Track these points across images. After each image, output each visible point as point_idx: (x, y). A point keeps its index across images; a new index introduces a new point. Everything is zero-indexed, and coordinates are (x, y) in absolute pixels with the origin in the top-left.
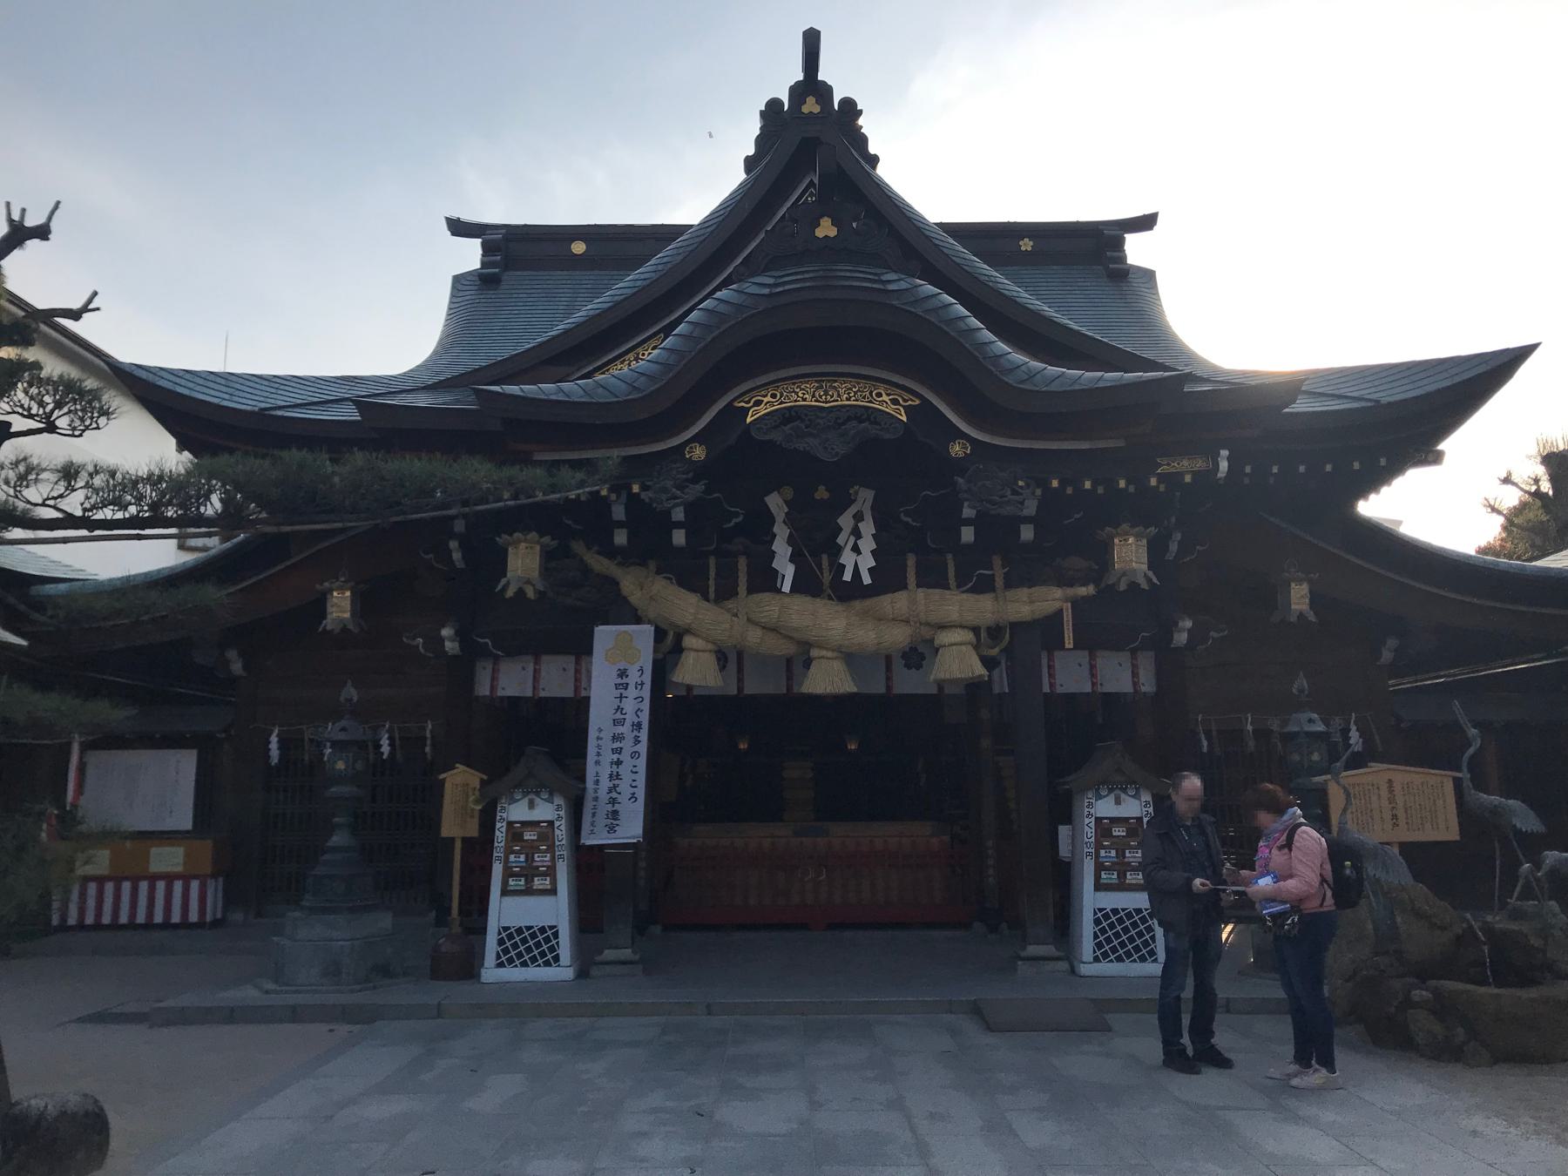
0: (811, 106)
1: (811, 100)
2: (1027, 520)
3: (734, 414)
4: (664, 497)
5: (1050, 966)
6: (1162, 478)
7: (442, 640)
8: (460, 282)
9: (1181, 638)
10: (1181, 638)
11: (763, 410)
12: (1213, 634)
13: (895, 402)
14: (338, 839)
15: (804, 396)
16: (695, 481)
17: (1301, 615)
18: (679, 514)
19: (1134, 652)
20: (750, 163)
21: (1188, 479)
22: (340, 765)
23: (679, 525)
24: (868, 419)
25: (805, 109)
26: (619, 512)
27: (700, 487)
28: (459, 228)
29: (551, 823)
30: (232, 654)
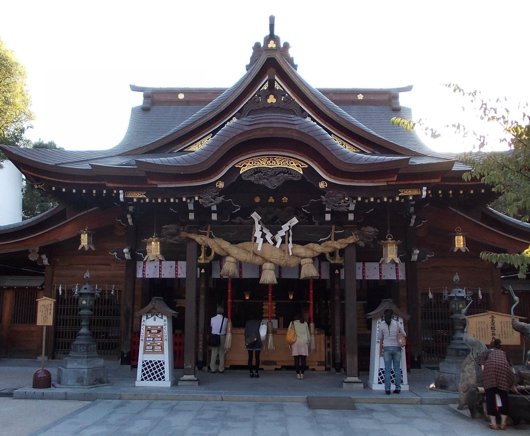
0: (272, 44)
1: (272, 42)
2: (351, 212)
4: (207, 202)
5: (356, 385)
6: (401, 197)
7: (124, 254)
8: (135, 111)
9: (415, 258)
10: (415, 258)
11: (246, 168)
12: (428, 256)
13: (298, 166)
14: (84, 330)
15: (263, 164)
17: (459, 250)
18: (214, 208)
20: (248, 67)
21: (411, 198)
22: (84, 302)
23: (214, 212)
24: (287, 173)
25: (270, 46)
26: (191, 207)
27: (221, 198)
28: (135, 89)
29: (162, 327)
30: (44, 257)
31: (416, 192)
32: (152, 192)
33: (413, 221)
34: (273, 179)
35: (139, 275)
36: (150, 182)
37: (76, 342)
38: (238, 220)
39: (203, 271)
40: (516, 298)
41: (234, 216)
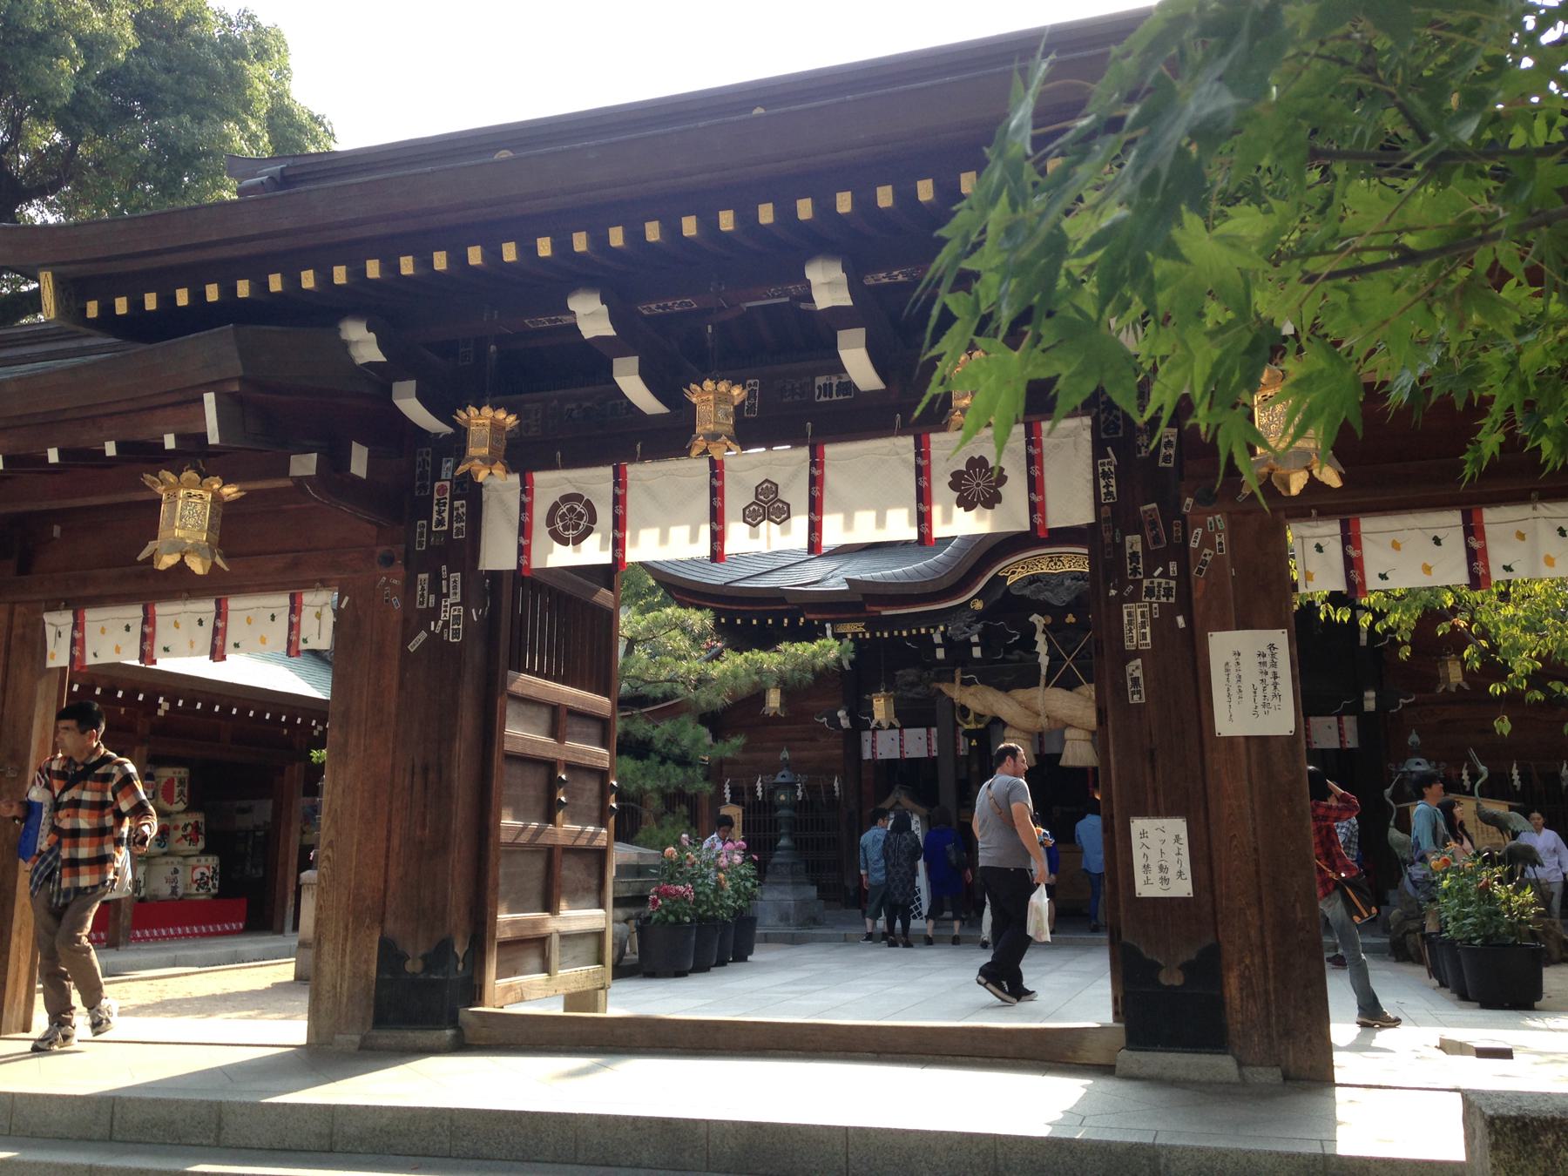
3: (998, 580)
9: (1370, 705)
10: (1370, 705)
11: (1016, 577)
14: (783, 842)
15: (1043, 568)
16: (977, 622)
18: (975, 639)
19: (1339, 716)
22: (783, 798)
23: (976, 645)
32: (874, 623)
35: (867, 755)
36: (869, 608)
37: (775, 860)
38: (1016, 655)
39: (974, 743)
40: (1483, 768)
41: (1009, 649)
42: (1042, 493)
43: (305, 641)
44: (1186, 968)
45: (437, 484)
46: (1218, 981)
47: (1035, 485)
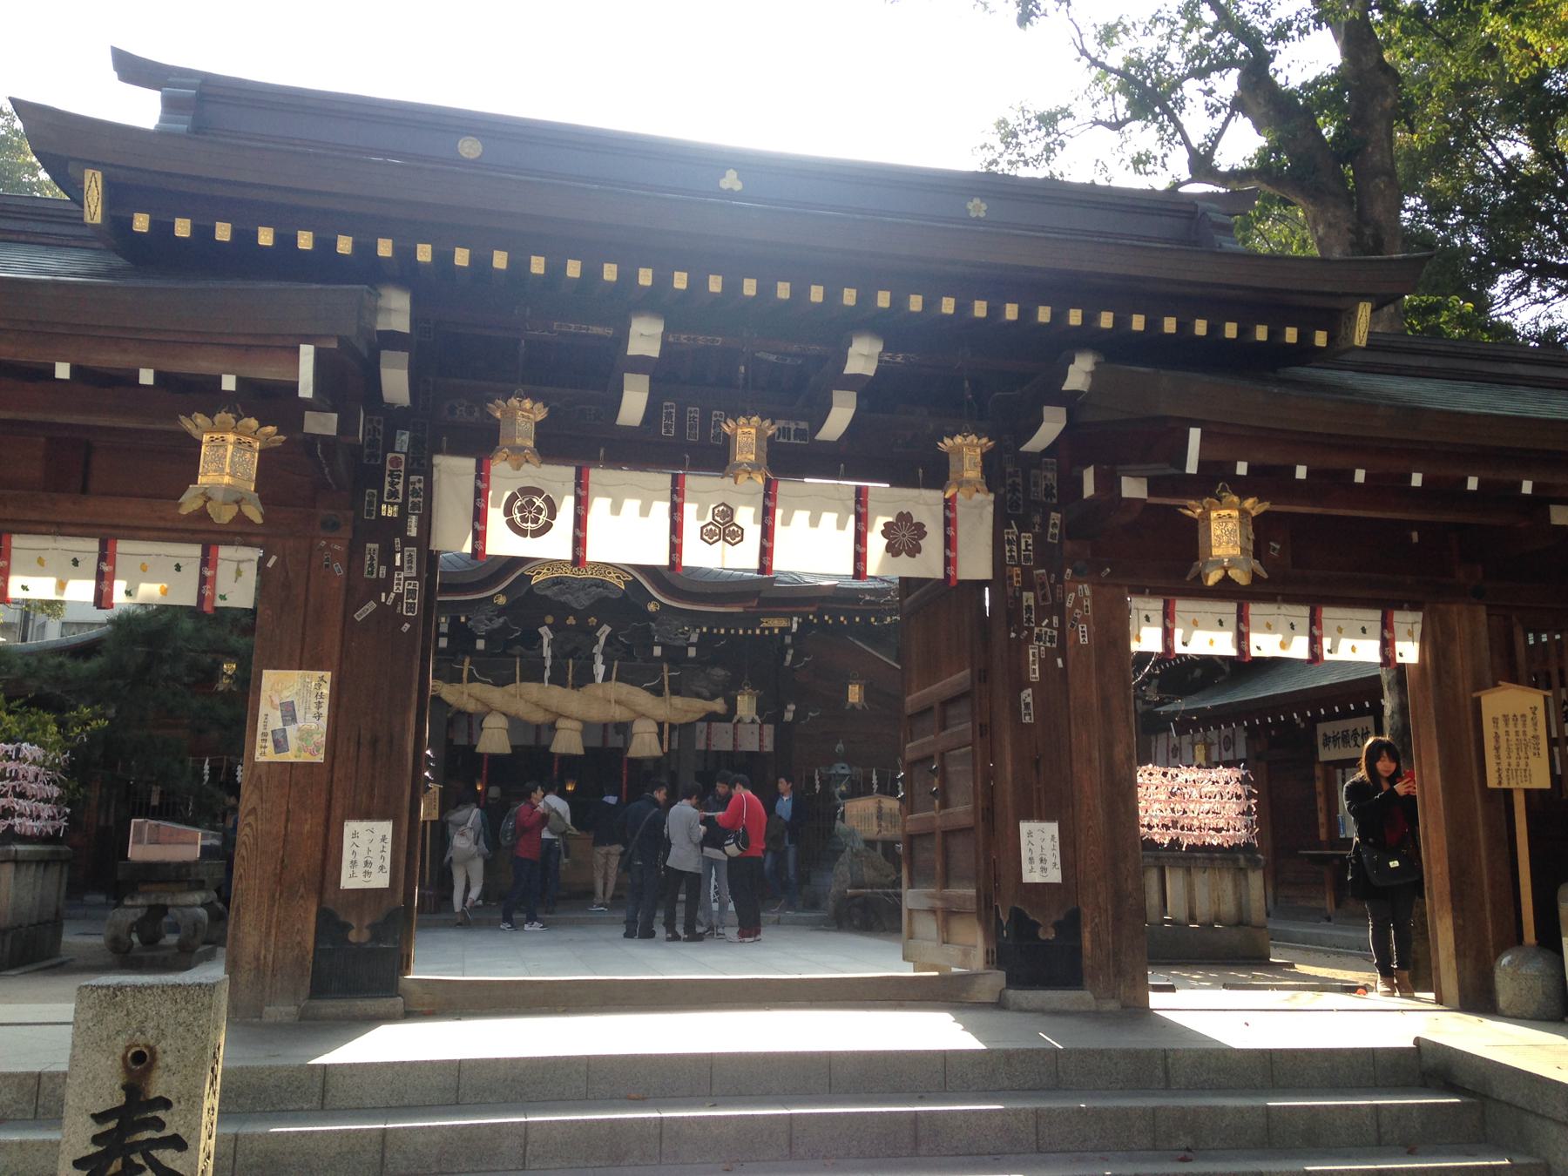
2: (692, 645)
6: (763, 630)
9: (789, 716)
10: (789, 716)
11: (541, 577)
17: (853, 706)
26: (444, 628)
31: (783, 623)
33: (789, 658)
34: (581, 594)
42: (955, 550)
43: (223, 597)
44: (1058, 926)
45: (390, 456)
46: (1078, 935)
47: (949, 542)
